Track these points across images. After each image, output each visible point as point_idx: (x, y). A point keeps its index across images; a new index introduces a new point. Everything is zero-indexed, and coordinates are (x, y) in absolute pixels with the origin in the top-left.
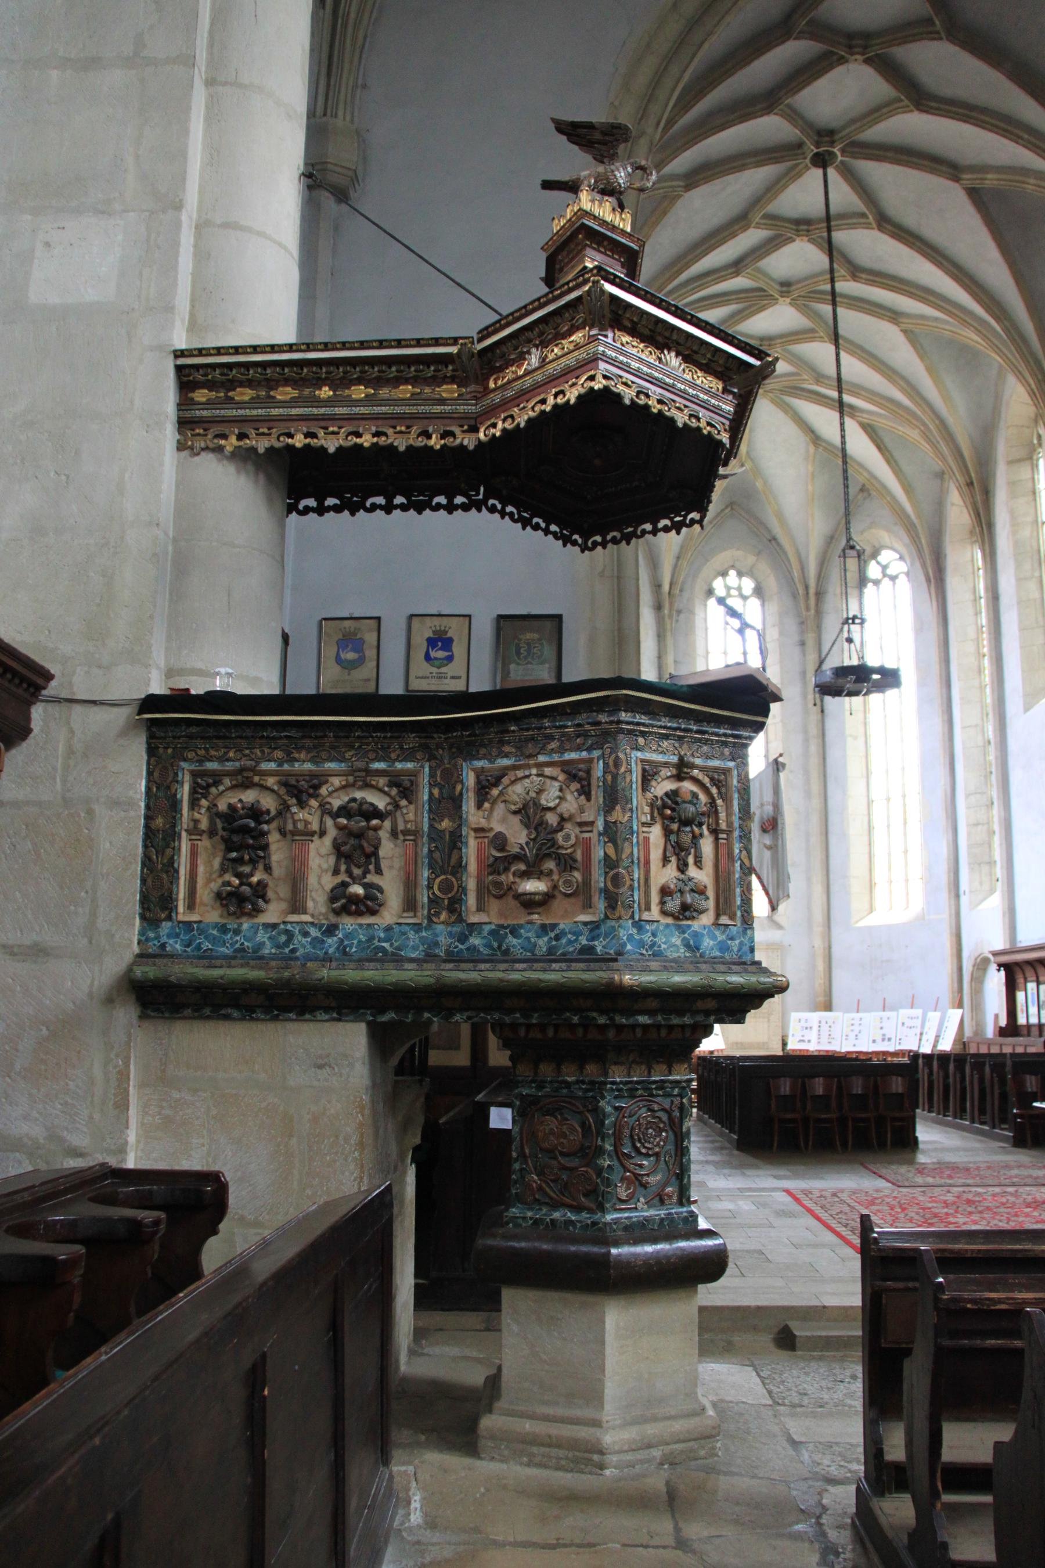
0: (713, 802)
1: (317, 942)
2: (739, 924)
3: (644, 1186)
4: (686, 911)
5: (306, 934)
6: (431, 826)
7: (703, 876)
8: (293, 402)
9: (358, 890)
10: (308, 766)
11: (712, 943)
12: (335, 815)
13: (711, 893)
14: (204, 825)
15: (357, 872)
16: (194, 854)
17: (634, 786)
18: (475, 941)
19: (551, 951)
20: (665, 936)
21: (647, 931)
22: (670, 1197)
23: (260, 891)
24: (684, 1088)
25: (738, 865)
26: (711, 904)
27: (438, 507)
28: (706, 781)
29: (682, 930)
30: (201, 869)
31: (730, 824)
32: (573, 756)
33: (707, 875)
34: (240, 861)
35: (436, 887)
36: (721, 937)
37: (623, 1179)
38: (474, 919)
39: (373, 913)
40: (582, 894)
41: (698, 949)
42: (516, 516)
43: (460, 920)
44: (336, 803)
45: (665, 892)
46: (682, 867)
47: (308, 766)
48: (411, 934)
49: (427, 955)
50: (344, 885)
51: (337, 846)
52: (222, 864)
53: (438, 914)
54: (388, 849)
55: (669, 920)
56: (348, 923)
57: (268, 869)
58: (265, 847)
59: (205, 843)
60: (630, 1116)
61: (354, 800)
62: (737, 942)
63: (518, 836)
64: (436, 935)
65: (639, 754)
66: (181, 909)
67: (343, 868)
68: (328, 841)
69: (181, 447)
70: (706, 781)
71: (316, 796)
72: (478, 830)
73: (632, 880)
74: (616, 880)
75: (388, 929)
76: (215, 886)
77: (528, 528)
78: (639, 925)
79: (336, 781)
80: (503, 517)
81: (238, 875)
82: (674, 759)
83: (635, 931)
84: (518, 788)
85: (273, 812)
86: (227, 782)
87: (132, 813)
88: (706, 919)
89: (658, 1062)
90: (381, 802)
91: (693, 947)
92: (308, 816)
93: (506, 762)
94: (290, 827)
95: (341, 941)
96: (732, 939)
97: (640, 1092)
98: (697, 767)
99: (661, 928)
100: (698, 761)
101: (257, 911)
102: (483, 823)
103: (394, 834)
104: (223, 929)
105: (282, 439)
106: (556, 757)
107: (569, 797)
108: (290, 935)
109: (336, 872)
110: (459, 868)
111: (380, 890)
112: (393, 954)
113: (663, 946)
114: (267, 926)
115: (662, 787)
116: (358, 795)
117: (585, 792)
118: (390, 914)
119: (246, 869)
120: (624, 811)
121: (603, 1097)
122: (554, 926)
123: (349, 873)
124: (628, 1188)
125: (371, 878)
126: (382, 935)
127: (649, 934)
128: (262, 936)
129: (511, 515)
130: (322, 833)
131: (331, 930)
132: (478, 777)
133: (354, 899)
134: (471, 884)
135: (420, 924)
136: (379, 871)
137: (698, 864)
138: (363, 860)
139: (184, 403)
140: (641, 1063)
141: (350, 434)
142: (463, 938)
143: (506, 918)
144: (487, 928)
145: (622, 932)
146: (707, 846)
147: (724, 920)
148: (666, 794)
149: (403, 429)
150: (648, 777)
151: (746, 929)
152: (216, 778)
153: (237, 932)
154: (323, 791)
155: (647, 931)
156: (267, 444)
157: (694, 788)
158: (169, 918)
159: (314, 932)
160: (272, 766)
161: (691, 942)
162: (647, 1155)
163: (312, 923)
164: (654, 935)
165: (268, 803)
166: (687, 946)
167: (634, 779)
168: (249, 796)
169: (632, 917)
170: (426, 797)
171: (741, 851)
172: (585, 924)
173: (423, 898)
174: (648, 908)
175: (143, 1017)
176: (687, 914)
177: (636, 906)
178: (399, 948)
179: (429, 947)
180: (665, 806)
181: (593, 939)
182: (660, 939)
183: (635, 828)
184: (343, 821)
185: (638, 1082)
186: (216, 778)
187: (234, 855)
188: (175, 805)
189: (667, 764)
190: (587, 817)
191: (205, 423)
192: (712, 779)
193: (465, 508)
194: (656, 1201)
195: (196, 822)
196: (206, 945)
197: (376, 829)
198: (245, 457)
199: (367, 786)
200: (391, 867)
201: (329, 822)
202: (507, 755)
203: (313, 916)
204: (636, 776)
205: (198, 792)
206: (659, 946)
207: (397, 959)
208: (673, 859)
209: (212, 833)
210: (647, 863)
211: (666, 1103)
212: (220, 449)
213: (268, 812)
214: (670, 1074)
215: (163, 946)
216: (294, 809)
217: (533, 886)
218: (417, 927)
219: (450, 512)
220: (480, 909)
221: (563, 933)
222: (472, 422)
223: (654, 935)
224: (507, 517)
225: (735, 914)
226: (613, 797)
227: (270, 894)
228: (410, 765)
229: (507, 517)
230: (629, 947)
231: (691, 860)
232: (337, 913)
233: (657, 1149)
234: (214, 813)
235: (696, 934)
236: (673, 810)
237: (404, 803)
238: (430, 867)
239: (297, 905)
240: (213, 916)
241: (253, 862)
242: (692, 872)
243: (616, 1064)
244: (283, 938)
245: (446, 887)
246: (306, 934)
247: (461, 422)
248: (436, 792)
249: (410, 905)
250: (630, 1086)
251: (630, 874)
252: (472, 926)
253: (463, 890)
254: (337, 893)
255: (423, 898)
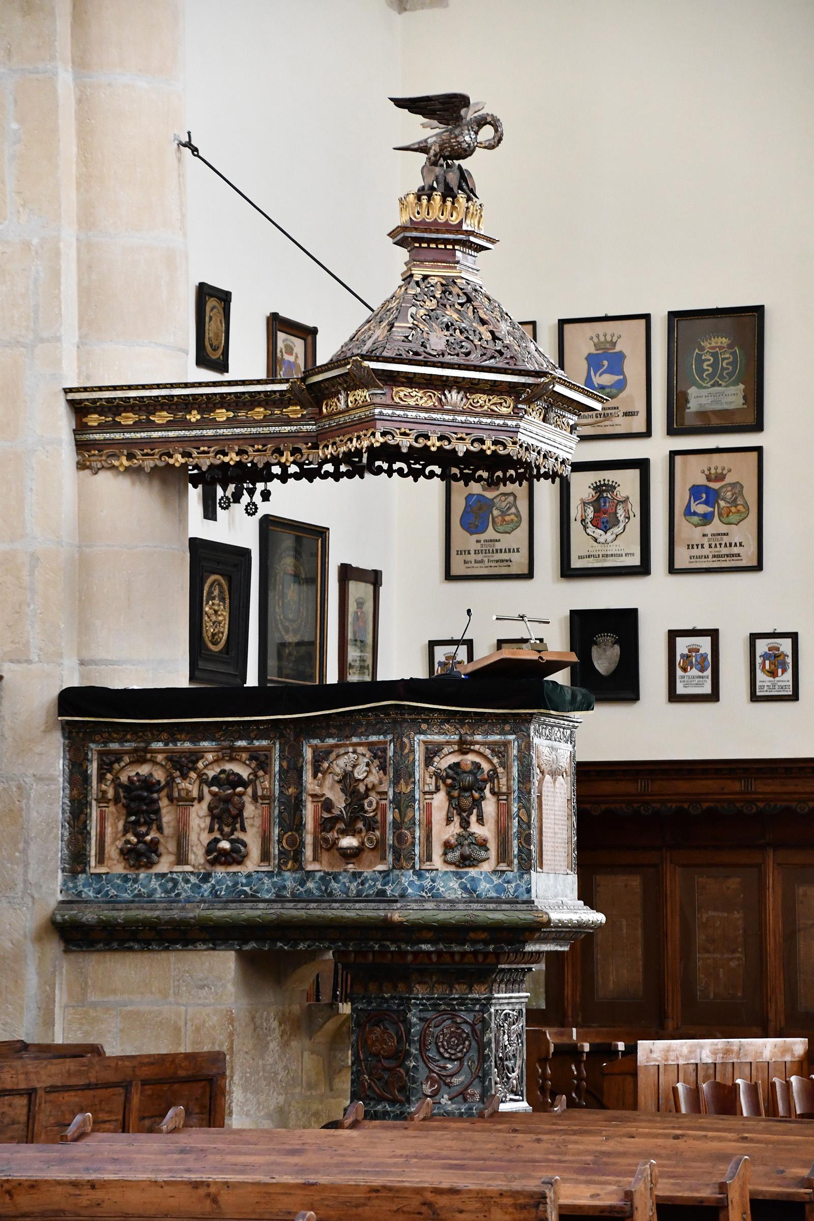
0: (494, 770)
1: (196, 887)
2: (516, 870)
3: (448, 1085)
4: (467, 861)
5: (187, 881)
6: (281, 792)
7: (485, 831)
8: (169, 426)
9: (225, 845)
10: (187, 745)
11: (488, 886)
12: (210, 785)
13: (492, 846)
14: (110, 794)
15: (227, 829)
16: (102, 819)
17: (417, 763)
18: (310, 885)
19: (359, 893)
20: (443, 881)
21: (428, 878)
22: (473, 1095)
23: (154, 847)
24: (485, 1005)
25: (516, 822)
26: (493, 853)
27: (326, 475)
28: (488, 752)
29: (459, 876)
30: (109, 830)
31: (509, 787)
32: (373, 738)
33: (489, 830)
34: (137, 823)
35: (284, 841)
36: (496, 880)
37: (428, 1078)
38: (310, 867)
39: (240, 863)
40: (379, 847)
41: (475, 892)
42: (406, 471)
43: (301, 868)
44: (211, 773)
45: (448, 847)
46: (465, 824)
47: (187, 745)
48: (266, 880)
49: (278, 896)
50: (216, 841)
51: (210, 809)
52: (125, 826)
53: (286, 863)
54: (250, 810)
55: (452, 868)
56: (220, 871)
57: (160, 829)
58: (158, 811)
59: (111, 809)
60: (435, 1027)
61: (223, 771)
62: (513, 885)
63: (340, 802)
64: (285, 880)
65: (422, 737)
66: (93, 863)
67: (216, 827)
68: (205, 805)
69: (81, 466)
70: (488, 752)
71: (195, 769)
72: (314, 796)
73: (414, 838)
74: (400, 838)
75: (249, 876)
76: (119, 844)
77: (422, 479)
78: (419, 874)
79: (210, 757)
80: (390, 476)
81: (136, 835)
82: (457, 738)
83: (416, 878)
84: (342, 762)
85: (163, 783)
86: (127, 759)
87: (53, 787)
88: (486, 867)
89: (459, 983)
90: (244, 772)
91: (470, 890)
92: (190, 786)
93: (331, 741)
94: (176, 794)
95: (214, 886)
96: (508, 882)
97: (443, 1007)
98: (477, 743)
99: (440, 875)
100: (478, 738)
101: (150, 864)
102: (318, 791)
103: (255, 798)
104: (125, 879)
105: (163, 459)
106: (363, 739)
107: (374, 771)
108: (175, 883)
109: (211, 830)
110: (299, 826)
111: (245, 845)
112: (252, 896)
113: (441, 889)
114: (158, 875)
115: (444, 762)
116: (228, 767)
117: (383, 768)
118: (252, 864)
119: (143, 829)
120: (407, 784)
121: (410, 1011)
122: (361, 873)
123: (221, 830)
124: (432, 1086)
125: (238, 835)
126: (244, 881)
127: (429, 880)
128: (154, 884)
129: (400, 472)
130: (201, 799)
131: (206, 878)
132: (314, 752)
133: (223, 852)
134: (309, 839)
135: (272, 872)
136: (243, 829)
137: (481, 820)
138: (230, 820)
139: (80, 429)
140: (443, 983)
141: (217, 453)
142: (302, 883)
143: (333, 867)
144: (318, 875)
145: (403, 879)
146: (489, 806)
147: (503, 866)
148: (450, 767)
149: (260, 447)
150: (432, 752)
151: (523, 874)
152: (118, 756)
153: (135, 881)
154: (200, 765)
155: (428, 878)
156: (152, 464)
157: (477, 759)
158: (84, 871)
159: (193, 879)
160: (160, 745)
161: (468, 886)
162: (450, 1060)
163: (192, 873)
164: (433, 881)
165: (159, 775)
166: (464, 888)
167: (417, 758)
168: (144, 770)
169: (413, 867)
170: (277, 769)
171: (519, 809)
172: (380, 872)
173: (275, 850)
174: (429, 859)
175: (66, 951)
176: (467, 863)
177: (417, 858)
178: (257, 891)
179: (279, 890)
180: (448, 776)
181: (384, 884)
182: (440, 885)
183: (417, 796)
184: (215, 789)
185: (438, 999)
186: (118, 756)
187: (133, 818)
188: (86, 779)
189: (448, 743)
190: (384, 788)
191: (99, 446)
192: (493, 751)
193: (350, 475)
194: (460, 1098)
195: (104, 792)
196: (113, 892)
197: (241, 795)
198: (134, 471)
199: (232, 759)
200: (252, 825)
201: (206, 789)
202: (331, 736)
203: (194, 866)
204: (419, 755)
205: (104, 769)
206: (438, 889)
207: (254, 899)
208: (457, 819)
209: (116, 800)
210: (429, 823)
211: (469, 1018)
212: (113, 467)
213: (159, 782)
214: (471, 992)
215: (79, 894)
216: (178, 780)
217: (348, 842)
218: (270, 874)
219: (337, 480)
220: (315, 859)
221: (366, 880)
222: (315, 441)
223: (433, 881)
224: (395, 474)
225: (512, 862)
226: (403, 773)
227: (161, 849)
228: (264, 743)
229: (395, 474)
230: (410, 891)
231: (473, 818)
232: (213, 863)
233: (459, 1055)
234: (117, 784)
235: (473, 879)
236: (453, 779)
237: (261, 773)
238: (280, 825)
239: (181, 859)
240: (119, 868)
241: (148, 824)
242: (475, 828)
243: (419, 983)
244: (170, 885)
245: (292, 842)
246: (187, 881)
247: (306, 440)
248: (285, 764)
249: (265, 856)
250: (432, 1001)
251: (413, 834)
252: (310, 874)
253: (302, 844)
254: (211, 848)
255: (275, 850)
